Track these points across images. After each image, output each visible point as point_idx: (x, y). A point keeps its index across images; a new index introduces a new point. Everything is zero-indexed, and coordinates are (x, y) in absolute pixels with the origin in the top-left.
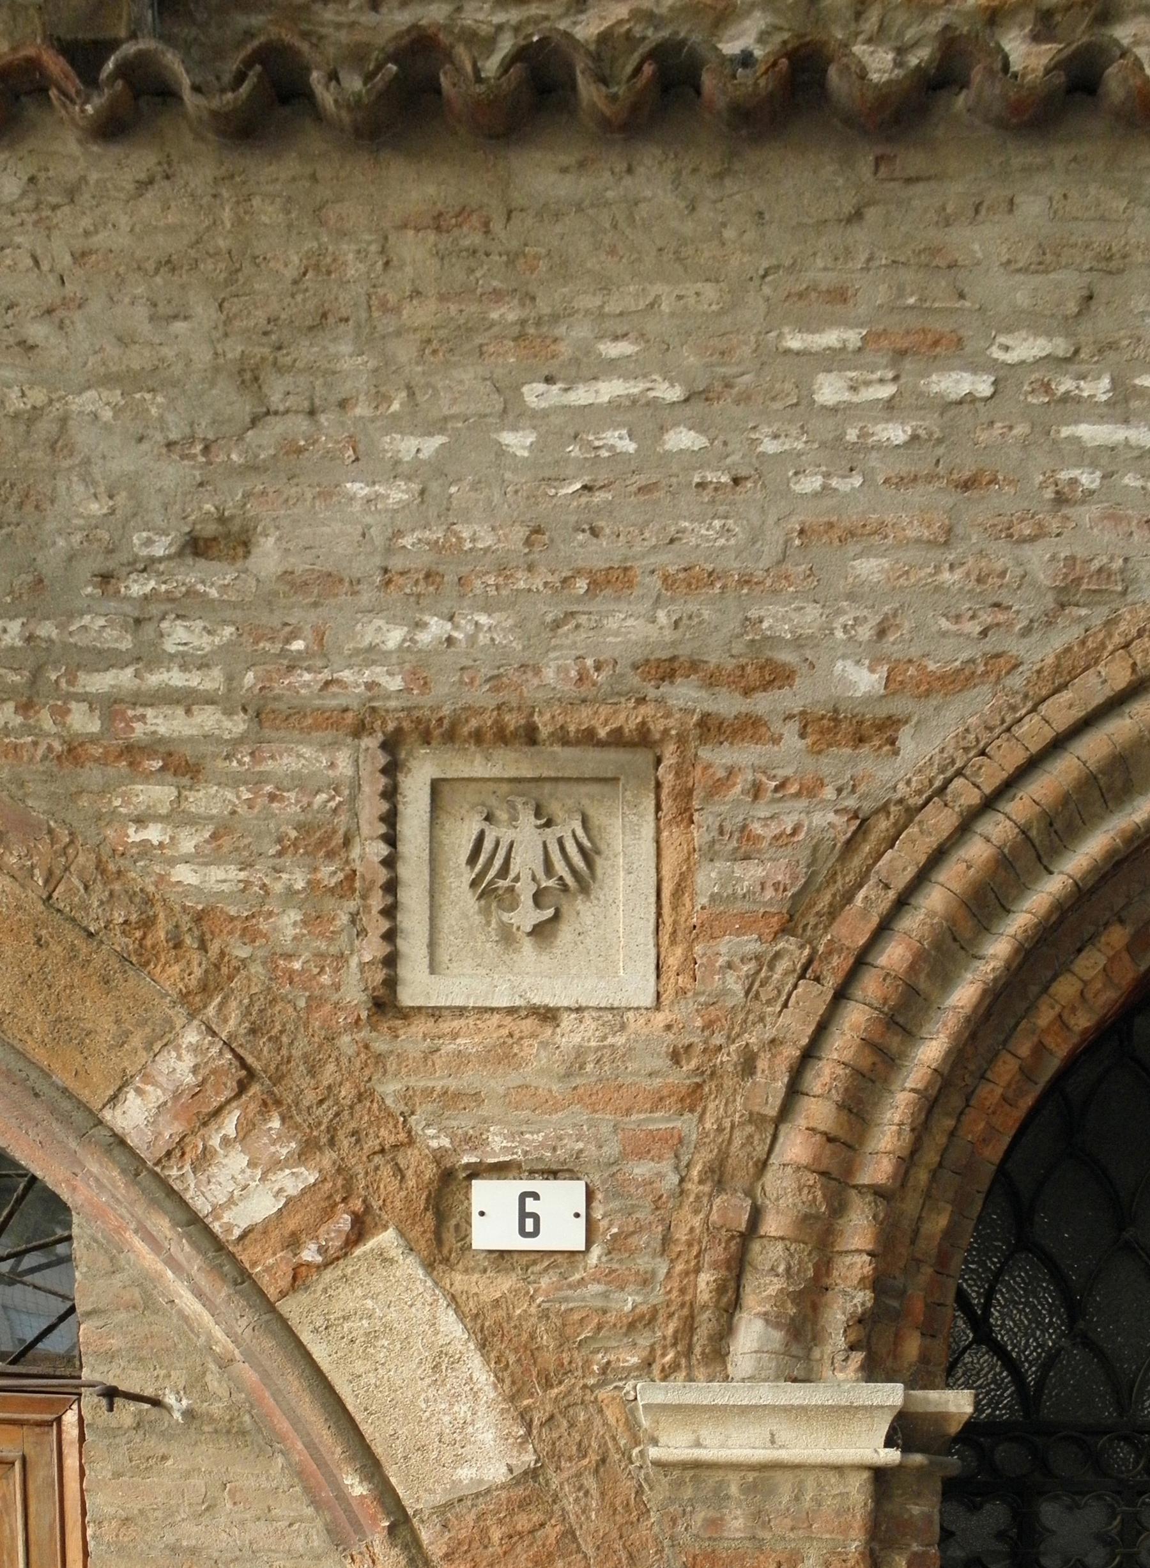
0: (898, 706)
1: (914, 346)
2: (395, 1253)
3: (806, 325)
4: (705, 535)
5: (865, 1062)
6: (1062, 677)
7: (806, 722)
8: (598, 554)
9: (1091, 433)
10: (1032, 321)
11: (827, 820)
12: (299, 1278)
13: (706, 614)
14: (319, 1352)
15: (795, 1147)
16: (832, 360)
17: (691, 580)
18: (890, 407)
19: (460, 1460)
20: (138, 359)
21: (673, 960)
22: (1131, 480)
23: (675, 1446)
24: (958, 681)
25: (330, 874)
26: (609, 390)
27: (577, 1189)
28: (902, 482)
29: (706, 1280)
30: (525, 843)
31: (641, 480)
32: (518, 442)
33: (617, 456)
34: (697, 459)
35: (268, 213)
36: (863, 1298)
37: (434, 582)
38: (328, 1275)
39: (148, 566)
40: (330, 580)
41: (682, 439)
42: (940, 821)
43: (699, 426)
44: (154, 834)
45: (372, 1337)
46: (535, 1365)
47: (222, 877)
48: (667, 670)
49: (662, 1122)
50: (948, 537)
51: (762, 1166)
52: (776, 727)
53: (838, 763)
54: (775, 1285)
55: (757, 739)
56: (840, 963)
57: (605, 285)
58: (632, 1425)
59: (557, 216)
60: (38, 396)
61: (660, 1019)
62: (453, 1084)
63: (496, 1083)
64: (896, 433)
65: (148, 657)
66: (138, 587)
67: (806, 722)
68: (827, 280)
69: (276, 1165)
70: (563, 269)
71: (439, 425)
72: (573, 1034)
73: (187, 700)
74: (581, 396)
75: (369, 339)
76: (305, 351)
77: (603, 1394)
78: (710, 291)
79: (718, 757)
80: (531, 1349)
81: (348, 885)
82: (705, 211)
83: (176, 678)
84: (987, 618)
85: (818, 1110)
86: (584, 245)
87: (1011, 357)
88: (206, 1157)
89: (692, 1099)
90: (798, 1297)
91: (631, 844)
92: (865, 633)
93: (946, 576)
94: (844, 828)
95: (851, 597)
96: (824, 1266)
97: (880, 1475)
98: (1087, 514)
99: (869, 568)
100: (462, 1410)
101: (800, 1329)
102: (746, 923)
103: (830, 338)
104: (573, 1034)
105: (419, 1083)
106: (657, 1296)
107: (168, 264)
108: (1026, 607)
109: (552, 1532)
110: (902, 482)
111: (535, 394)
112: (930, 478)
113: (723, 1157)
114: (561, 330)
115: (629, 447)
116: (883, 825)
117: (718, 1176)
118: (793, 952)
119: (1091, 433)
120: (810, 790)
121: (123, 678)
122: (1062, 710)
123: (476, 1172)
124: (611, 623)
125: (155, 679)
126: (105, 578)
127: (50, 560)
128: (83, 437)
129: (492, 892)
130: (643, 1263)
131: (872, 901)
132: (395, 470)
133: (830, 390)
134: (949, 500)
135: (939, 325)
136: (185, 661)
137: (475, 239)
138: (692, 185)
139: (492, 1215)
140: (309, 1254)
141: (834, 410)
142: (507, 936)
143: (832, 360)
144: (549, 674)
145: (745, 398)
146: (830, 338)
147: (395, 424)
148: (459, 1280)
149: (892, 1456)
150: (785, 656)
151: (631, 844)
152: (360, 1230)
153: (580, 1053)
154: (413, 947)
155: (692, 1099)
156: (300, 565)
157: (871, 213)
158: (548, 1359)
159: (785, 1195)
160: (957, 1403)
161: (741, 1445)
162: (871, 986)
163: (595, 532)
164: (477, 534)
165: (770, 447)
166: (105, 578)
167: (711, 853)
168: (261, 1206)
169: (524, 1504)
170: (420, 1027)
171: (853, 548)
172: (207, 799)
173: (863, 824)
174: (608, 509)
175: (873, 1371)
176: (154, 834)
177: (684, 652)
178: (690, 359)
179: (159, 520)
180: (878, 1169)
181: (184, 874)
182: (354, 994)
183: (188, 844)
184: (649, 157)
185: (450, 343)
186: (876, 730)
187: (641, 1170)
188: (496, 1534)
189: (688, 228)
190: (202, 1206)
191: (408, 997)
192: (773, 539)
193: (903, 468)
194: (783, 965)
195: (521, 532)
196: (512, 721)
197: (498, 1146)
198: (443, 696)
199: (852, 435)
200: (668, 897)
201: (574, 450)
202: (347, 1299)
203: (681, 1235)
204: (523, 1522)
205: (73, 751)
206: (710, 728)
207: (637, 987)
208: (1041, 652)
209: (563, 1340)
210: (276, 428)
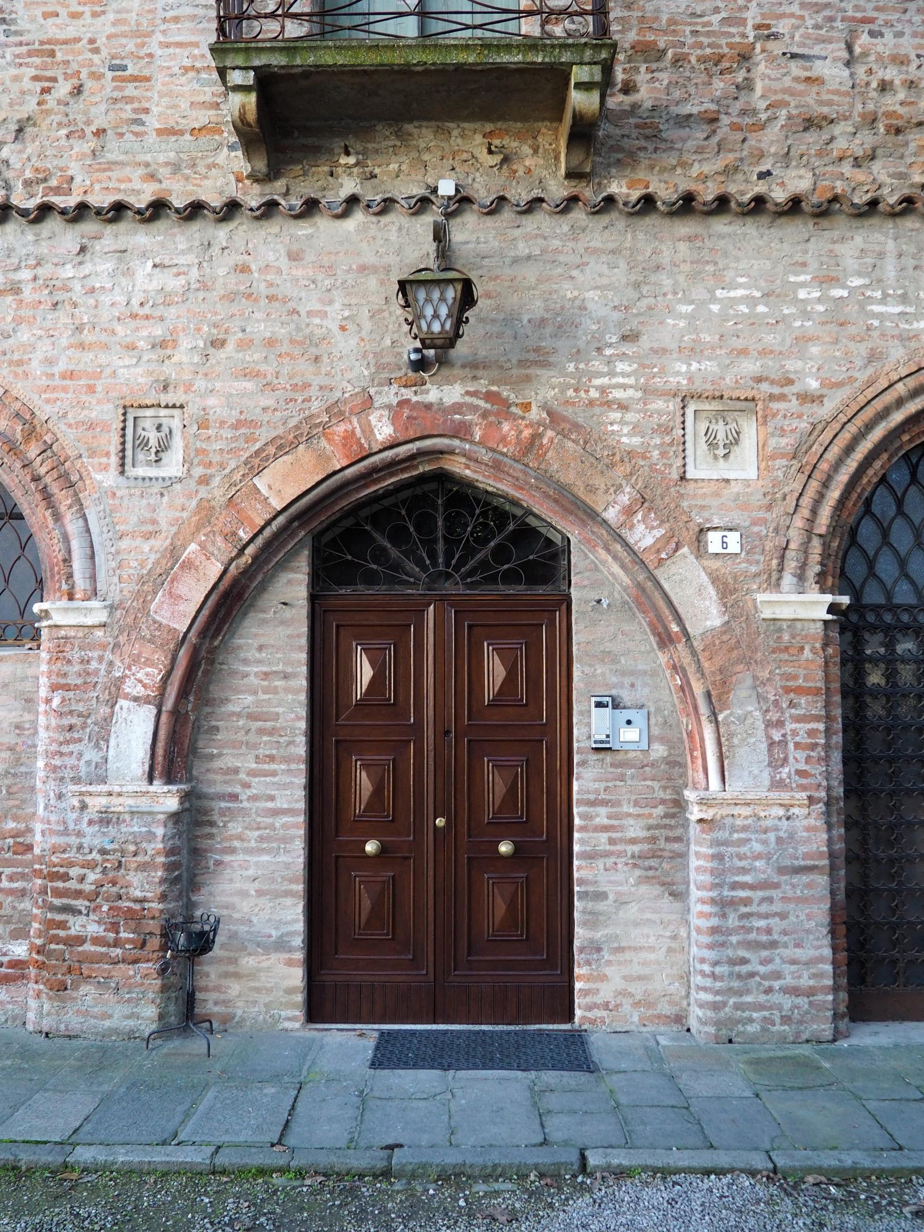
0: (825, 391)
1: (827, 280)
2: (688, 555)
3: (796, 274)
4: (770, 339)
5: (816, 497)
6: (870, 383)
7: (798, 396)
8: (739, 344)
9: (877, 308)
10: (860, 274)
11: (804, 425)
12: (661, 562)
13: (770, 363)
14: (666, 586)
15: (799, 522)
16: (803, 285)
17: (764, 353)
18: (819, 300)
19: (706, 619)
20: (605, 281)
21: (763, 466)
22: (888, 324)
23: (767, 613)
24: (839, 385)
25: (668, 439)
26: (740, 293)
27: (738, 534)
28: (823, 323)
29: (775, 562)
30: (720, 429)
31: (751, 321)
32: (715, 308)
33: (743, 314)
34: (765, 315)
35: (641, 236)
36: (817, 569)
37: (694, 351)
38: (669, 562)
39: (610, 345)
40: (664, 351)
41: (761, 309)
42: (836, 426)
43: (766, 305)
44: (616, 427)
45: (681, 581)
46: (727, 590)
47: (636, 441)
48: (759, 380)
49: (761, 514)
50: (836, 341)
51: (788, 527)
52: (790, 397)
53: (808, 408)
54: (794, 564)
55: (785, 401)
56: (809, 468)
57: (737, 259)
58: (756, 607)
59: (724, 238)
60: (576, 293)
61: (760, 483)
62: (703, 503)
63: (715, 502)
64: (821, 308)
65: (612, 374)
66: (608, 352)
67: (798, 396)
68: (800, 260)
69: (653, 528)
70: (726, 254)
71: (691, 302)
72: (735, 488)
73: (624, 387)
74: (732, 294)
75: (671, 275)
76: (653, 278)
77: (747, 597)
78: (767, 262)
79: (775, 406)
80: (726, 584)
81: (671, 444)
82: (765, 238)
83: (621, 380)
84: (848, 366)
85: (805, 512)
86: (732, 248)
87: (853, 285)
88: (632, 527)
89: (769, 508)
90: (800, 568)
91: (750, 431)
92: (814, 370)
93: (837, 354)
94: (809, 428)
95: (810, 359)
96: (806, 558)
97: (826, 622)
98: (875, 334)
99: (815, 350)
100: (707, 603)
101: (801, 577)
102: (783, 456)
103: (802, 278)
104: (735, 488)
105: (693, 502)
106: (761, 567)
107: (613, 252)
108: (859, 363)
109: (733, 641)
110: (823, 323)
111: (719, 293)
112: (832, 322)
113: (778, 525)
114: (725, 273)
115: (746, 311)
116: (820, 427)
117: (776, 530)
118: (796, 464)
119: (877, 308)
120: (800, 416)
121: (605, 381)
122: (870, 393)
123: (709, 529)
124: (744, 365)
125: (614, 381)
126: (599, 349)
127: (581, 344)
128: (590, 305)
129: (712, 445)
130: (757, 557)
131: (817, 449)
132: (681, 316)
133: (802, 294)
134: (837, 329)
135: (833, 274)
136: (623, 374)
137: (700, 244)
138: (762, 230)
139: (714, 541)
140: (663, 556)
141: (803, 301)
142: (716, 457)
143: (803, 285)
144: (728, 380)
145: (778, 296)
146: (802, 278)
147: (679, 301)
148: (706, 563)
149: (830, 617)
150: (792, 376)
151: (750, 431)
152: (678, 547)
153: (738, 494)
154: (690, 460)
155: (769, 508)
156: (655, 345)
157: (812, 239)
158: (731, 587)
159: (796, 537)
160: (845, 600)
161: (786, 613)
162: (817, 475)
163: (738, 337)
164: (706, 337)
165: (786, 312)
166: (599, 349)
167: (773, 435)
168: (649, 541)
169: (725, 632)
170: (692, 485)
171: (810, 344)
172: (630, 417)
173: (814, 426)
174: (742, 330)
175: (823, 591)
176: (616, 427)
177: (764, 375)
178: (763, 284)
179: (613, 330)
180: (822, 530)
181: (625, 440)
182: (675, 476)
183: (625, 431)
184: (749, 220)
185: (694, 276)
186: (818, 399)
187: (756, 529)
188: (717, 642)
189: (761, 243)
190: (631, 541)
191: (688, 476)
192: (788, 341)
193: (824, 319)
194: (793, 468)
195: (717, 337)
196: (717, 394)
197: (716, 522)
198: (698, 386)
199: (809, 309)
200: (761, 447)
201: (731, 312)
202: (674, 569)
203: (767, 548)
204: (725, 638)
205: (591, 403)
206: (772, 397)
207: (752, 474)
208: (863, 376)
209: (735, 580)
210: (644, 303)
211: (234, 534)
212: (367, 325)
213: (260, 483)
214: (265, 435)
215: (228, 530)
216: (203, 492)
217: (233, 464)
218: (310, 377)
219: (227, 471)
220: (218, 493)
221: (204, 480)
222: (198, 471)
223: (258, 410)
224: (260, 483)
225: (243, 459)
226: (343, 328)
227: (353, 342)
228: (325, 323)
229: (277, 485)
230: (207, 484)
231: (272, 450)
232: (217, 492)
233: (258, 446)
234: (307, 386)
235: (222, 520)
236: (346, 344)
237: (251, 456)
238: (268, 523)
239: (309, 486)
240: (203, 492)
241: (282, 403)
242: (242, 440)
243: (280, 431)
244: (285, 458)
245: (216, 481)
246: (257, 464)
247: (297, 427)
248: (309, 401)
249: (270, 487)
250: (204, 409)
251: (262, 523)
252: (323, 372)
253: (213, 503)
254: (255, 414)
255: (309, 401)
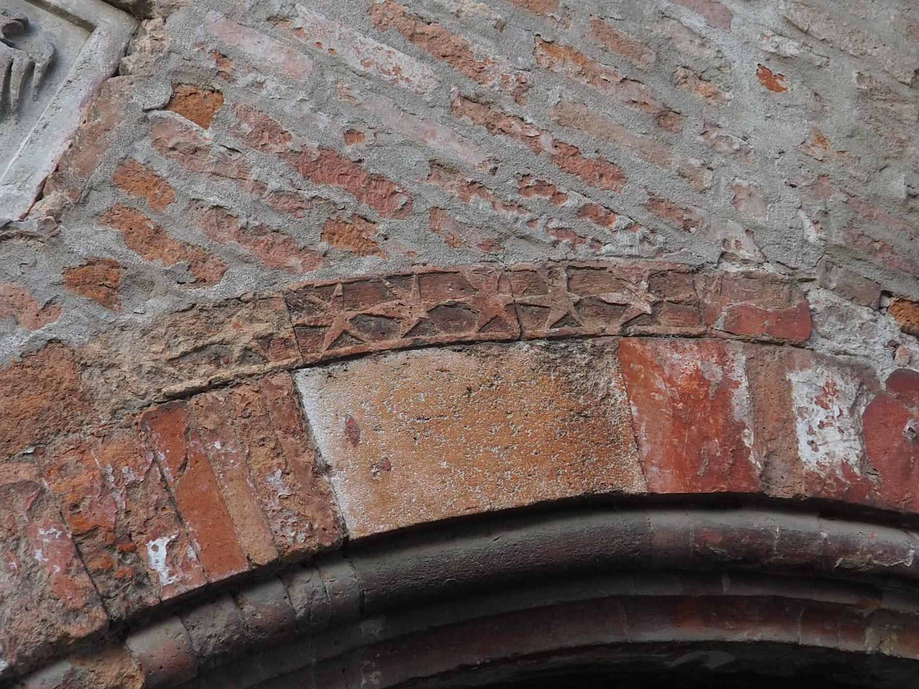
211: (125, 544)
212: (845, 113)
213: (323, 403)
214: (403, 246)
215: (103, 513)
216: (73, 322)
217: (242, 281)
218: (626, 155)
219: (212, 293)
220: (130, 353)
221: (101, 282)
222: (91, 239)
223: (414, 158)
224: (323, 403)
225: (294, 283)
226: (768, 79)
227: (792, 131)
228: (717, 36)
229: (384, 440)
230: (107, 302)
231: (413, 307)
232: (133, 346)
233: (366, 266)
234: (607, 171)
235: (104, 464)
236: (770, 127)
237: (325, 290)
238: (287, 567)
239: (506, 502)
240: (73, 322)
241: (507, 177)
242: (316, 217)
243: (468, 262)
244: (451, 358)
245: (150, 308)
246: (339, 326)
247: (532, 279)
248: (604, 221)
249: (352, 433)
250: (222, 57)
251: (265, 555)
252: (676, 159)
253: (93, 380)
254: (404, 167)
255: (604, 221)
